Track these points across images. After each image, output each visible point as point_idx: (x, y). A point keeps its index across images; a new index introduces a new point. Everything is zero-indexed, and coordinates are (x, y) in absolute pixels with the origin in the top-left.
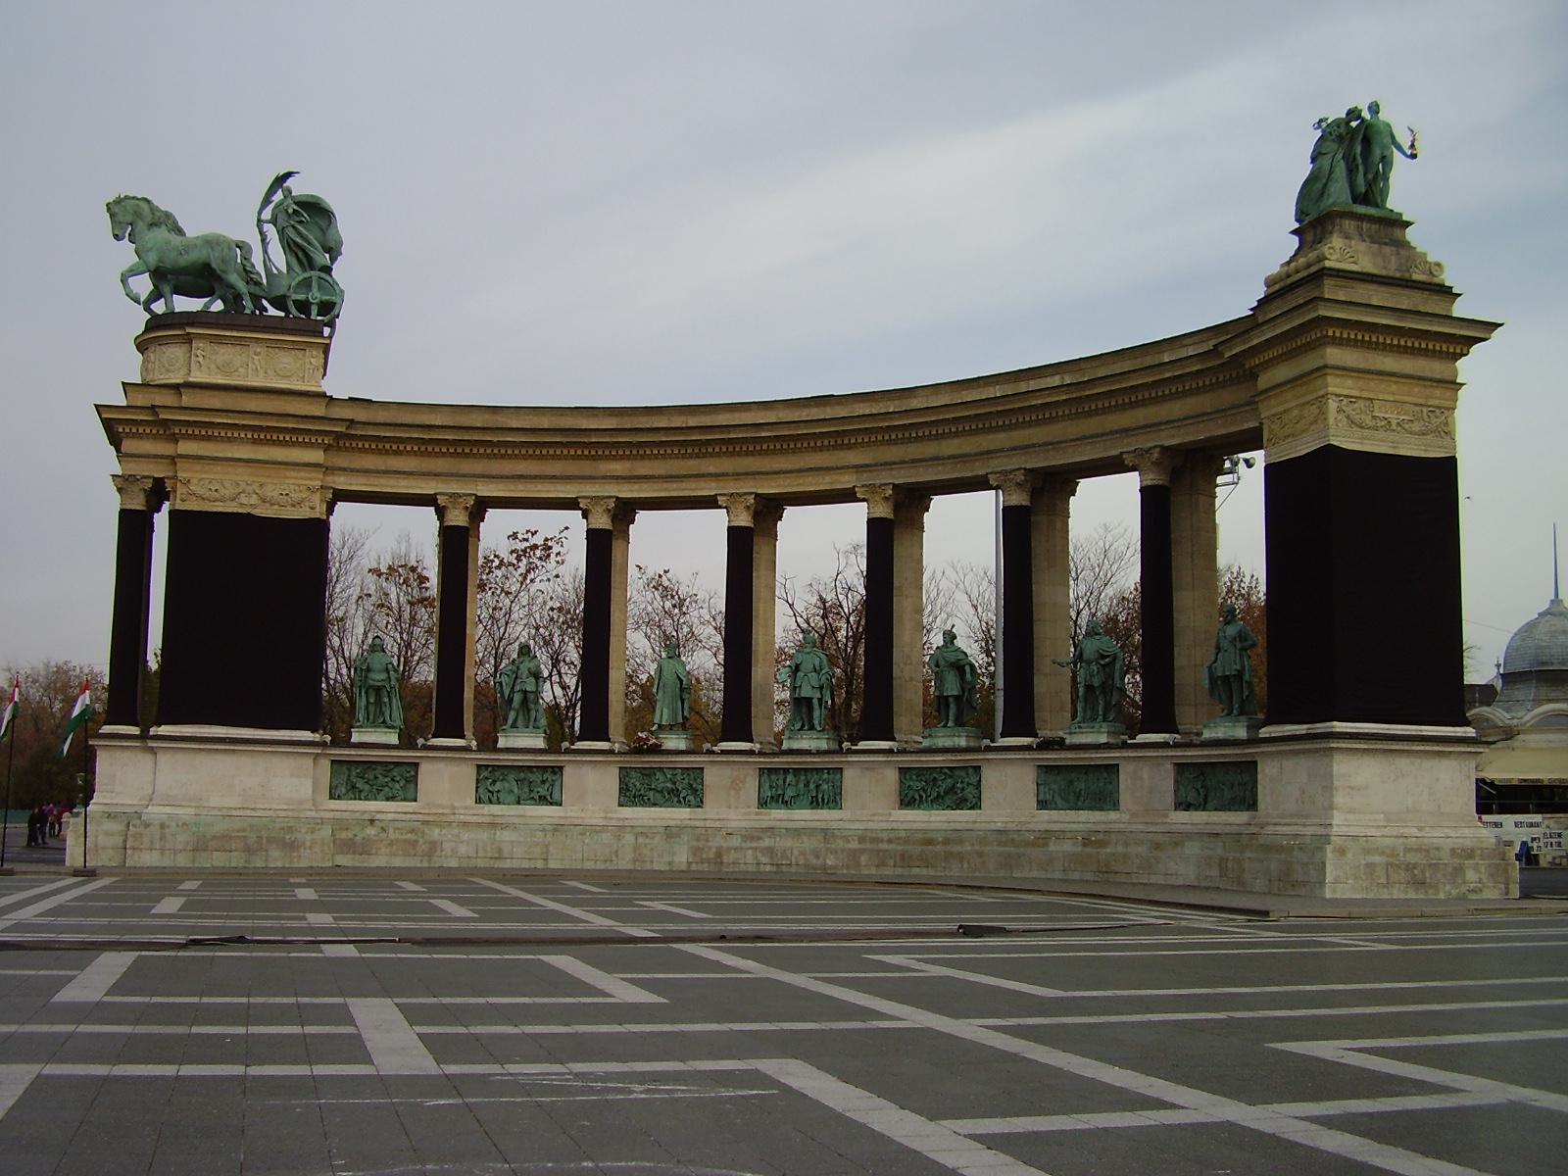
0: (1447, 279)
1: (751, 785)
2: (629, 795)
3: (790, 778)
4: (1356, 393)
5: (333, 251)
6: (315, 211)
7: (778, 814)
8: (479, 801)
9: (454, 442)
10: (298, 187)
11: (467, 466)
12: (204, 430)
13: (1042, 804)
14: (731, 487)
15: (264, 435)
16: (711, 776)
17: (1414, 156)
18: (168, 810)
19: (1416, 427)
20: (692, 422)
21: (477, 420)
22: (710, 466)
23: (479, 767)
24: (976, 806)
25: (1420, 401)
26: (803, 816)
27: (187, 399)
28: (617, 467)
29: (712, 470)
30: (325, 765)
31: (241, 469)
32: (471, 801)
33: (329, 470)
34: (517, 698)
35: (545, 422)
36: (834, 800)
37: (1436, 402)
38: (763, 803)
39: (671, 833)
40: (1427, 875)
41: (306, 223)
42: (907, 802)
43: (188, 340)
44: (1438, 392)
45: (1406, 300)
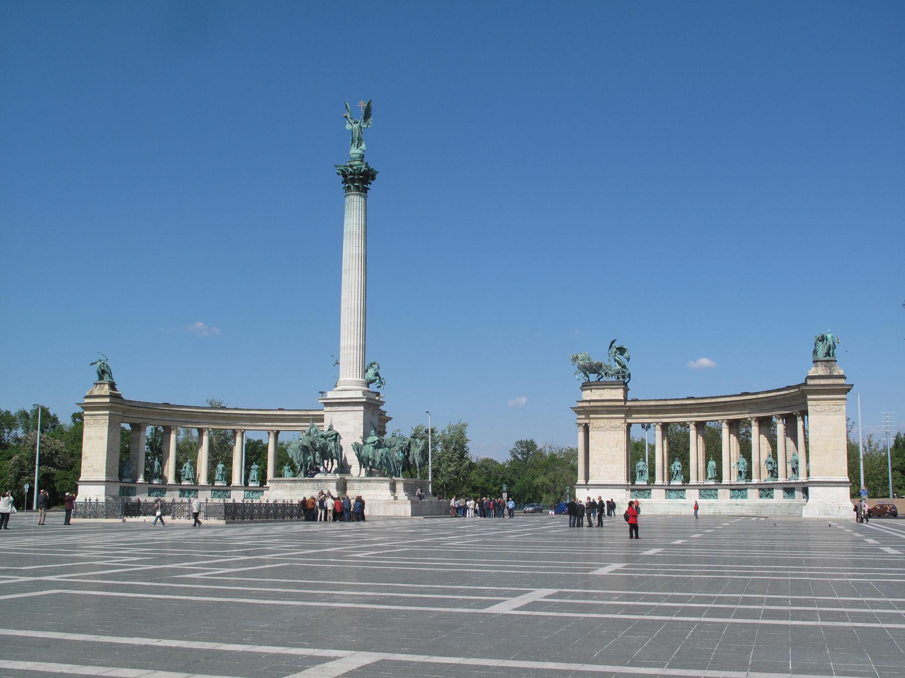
6: (622, 350)
7: (734, 501)
26: (739, 501)
27: (592, 404)
35: (678, 402)
36: (745, 497)
39: (710, 505)
43: (591, 389)
45: (830, 381)
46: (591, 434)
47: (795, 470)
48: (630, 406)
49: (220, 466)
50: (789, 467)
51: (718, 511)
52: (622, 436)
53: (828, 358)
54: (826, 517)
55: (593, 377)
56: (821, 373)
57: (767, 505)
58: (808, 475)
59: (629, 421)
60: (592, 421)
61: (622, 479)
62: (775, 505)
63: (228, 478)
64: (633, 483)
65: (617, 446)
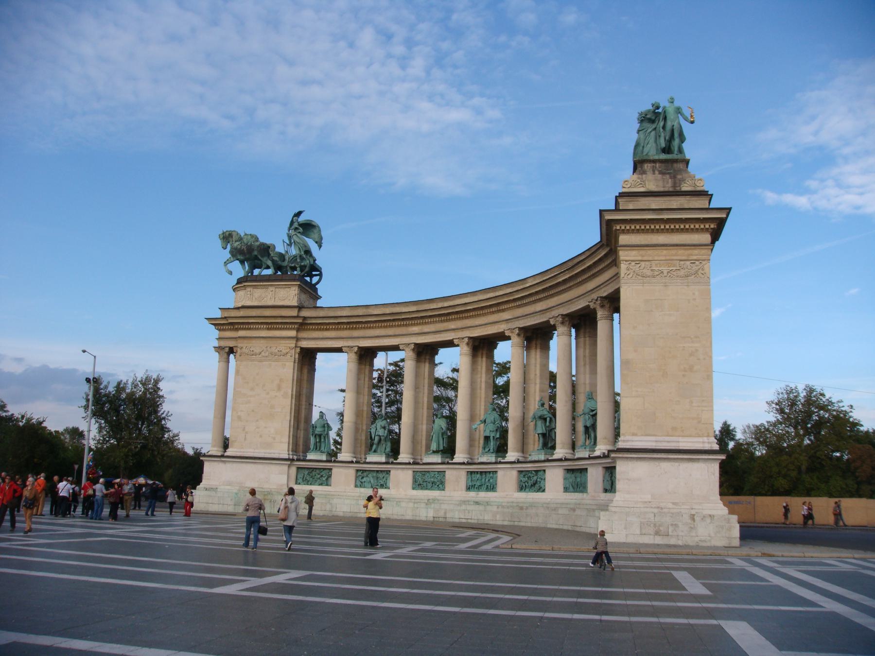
2: (418, 484)
3: (478, 476)
4: (640, 258)
7: (472, 494)
8: (356, 486)
9: (348, 323)
11: (356, 333)
12: (246, 326)
13: (566, 490)
15: (271, 326)
17: (692, 122)
18: (229, 487)
19: (682, 273)
20: (446, 304)
21: (360, 312)
22: (452, 325)
23: (357, 471)
25: (684, 258)
26: (483, 495)
27: (242, 313)
28: (416, 329)
29: (453, 327)
30: (293, 470)
31: (262, 341)
32: (353, 486)
33: (298, 339)
34: (377, 439)
36: (492, 488)
37: (695, 258)
38: (469, 488)
39: (429, 502)
40: (670, 530)
42: (522, 488)
44: (696, 252)
47: (590, 430)
48: (305, 318)
50: (580, 428)
51: (441, 514)
53: (663, 156)
54: (659, 540)
56: (652, 187)
57: (532, 505)
58: (617, 434)
59: (305, 344)
61: (282, 449)
62: (547, 506)
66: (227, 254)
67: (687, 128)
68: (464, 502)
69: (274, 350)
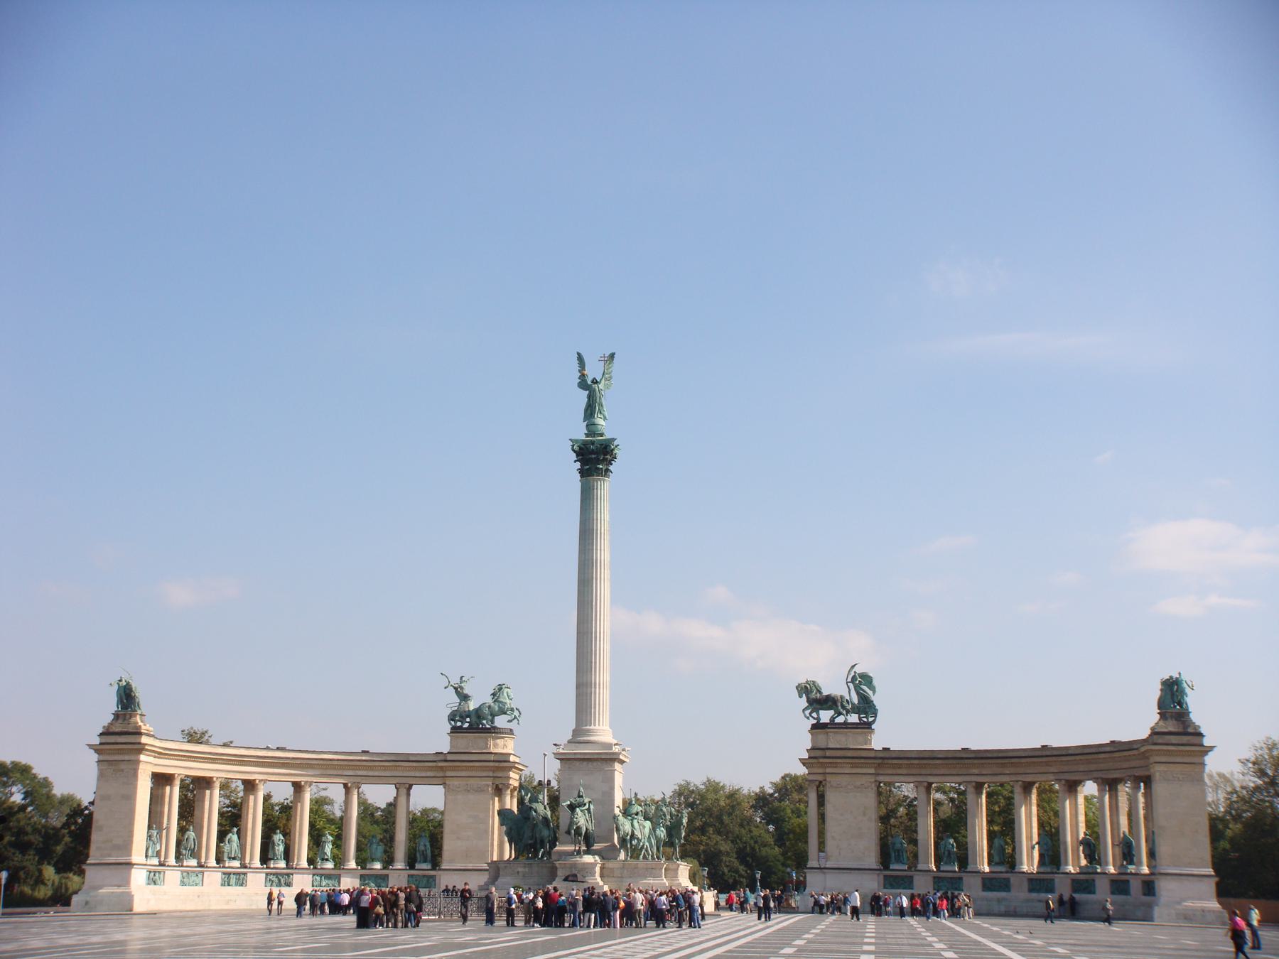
0: (1202, 731)
1: (1026, 885)
5: (874, 692)
6: (867, 679)
7: (1034, 895)
10: (858, 670)
11: (923, 772)
12: (835, 765)
13: (1113, 893)
14: (1014, 778)
15: (853, 766)
16: (1012, 880)
24: (1094, 893)
27: (828, 753)
28: (976, 771)
30: (882, 877)
33: (877, 774)
38: (1031, 890)
39: (999, 901)
41: (862, 681)
45: (1185, 739)
46: (830, 797)
49: (278, 837)
52: (870, 799)
55: (826, 716)
59: (881, 778)
60: (829, 778)
61: (872, 860)
63: (287, 855)
64: (886, 868)
65: (864, 814)
66: (803, 702)
67: (1188, 690)
68: (1027, 901)
69: (858, 783)
